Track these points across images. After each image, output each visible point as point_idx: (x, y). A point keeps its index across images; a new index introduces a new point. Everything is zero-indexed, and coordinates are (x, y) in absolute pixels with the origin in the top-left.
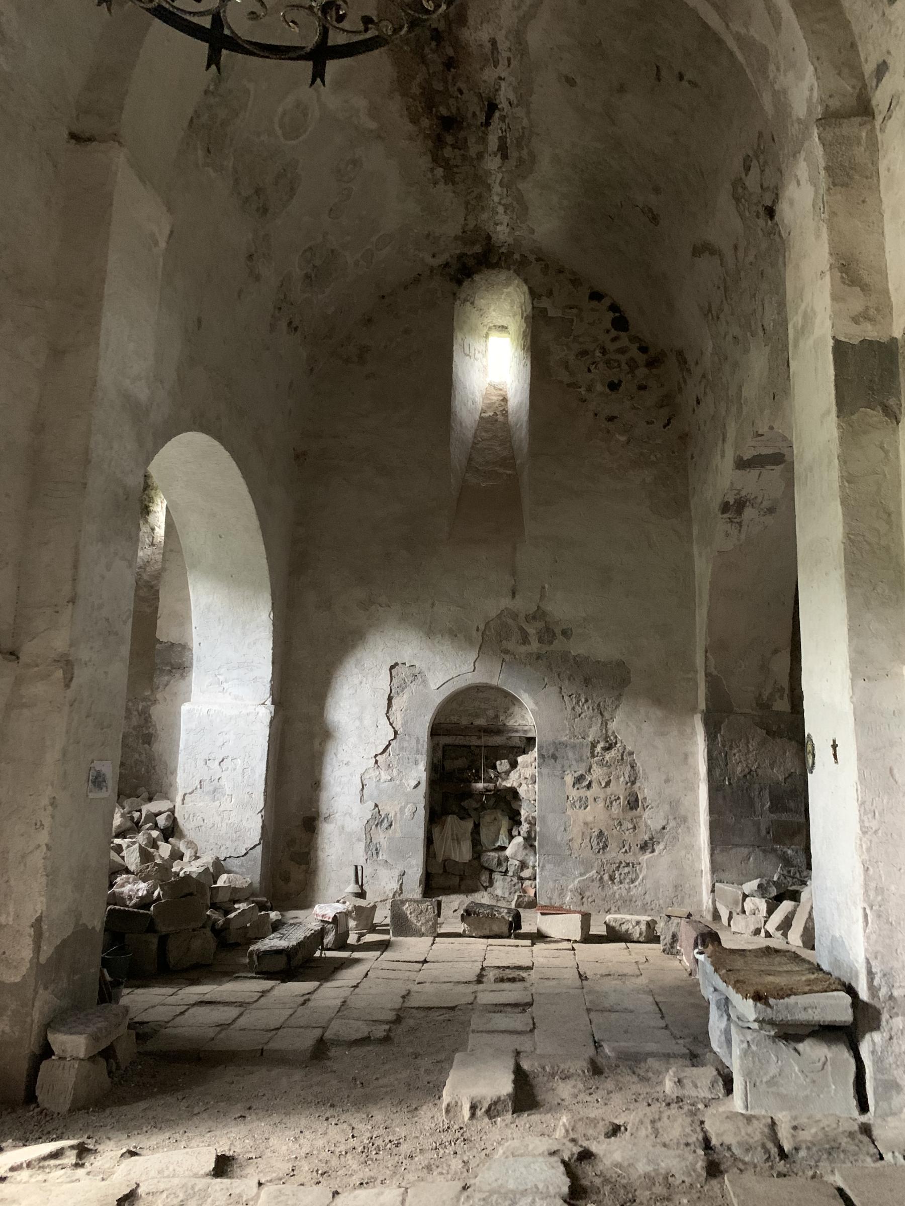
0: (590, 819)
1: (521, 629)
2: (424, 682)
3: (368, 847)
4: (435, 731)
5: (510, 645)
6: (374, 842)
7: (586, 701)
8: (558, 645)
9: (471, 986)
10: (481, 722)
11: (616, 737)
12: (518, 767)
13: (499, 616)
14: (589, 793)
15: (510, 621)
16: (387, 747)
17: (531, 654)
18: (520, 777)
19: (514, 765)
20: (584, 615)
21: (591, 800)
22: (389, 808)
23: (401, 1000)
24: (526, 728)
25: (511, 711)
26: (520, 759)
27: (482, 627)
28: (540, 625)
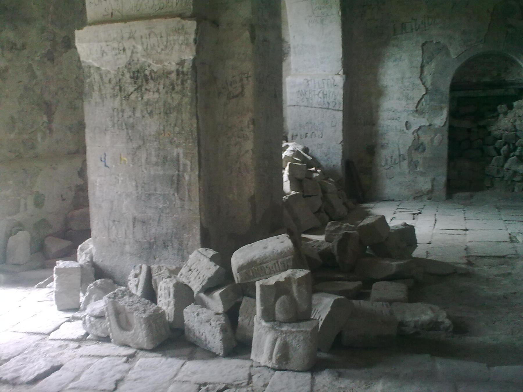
2: (448, 54)
3: (409, 163)
4: (454, 87)
6: (414, 160)
9: (506, 243)
10: (487, 79)
16: (421, 99)
18: (515, 116)
19: (511, 107)
22: (425, 139)
23: (465, 251)
26: (515, 104)
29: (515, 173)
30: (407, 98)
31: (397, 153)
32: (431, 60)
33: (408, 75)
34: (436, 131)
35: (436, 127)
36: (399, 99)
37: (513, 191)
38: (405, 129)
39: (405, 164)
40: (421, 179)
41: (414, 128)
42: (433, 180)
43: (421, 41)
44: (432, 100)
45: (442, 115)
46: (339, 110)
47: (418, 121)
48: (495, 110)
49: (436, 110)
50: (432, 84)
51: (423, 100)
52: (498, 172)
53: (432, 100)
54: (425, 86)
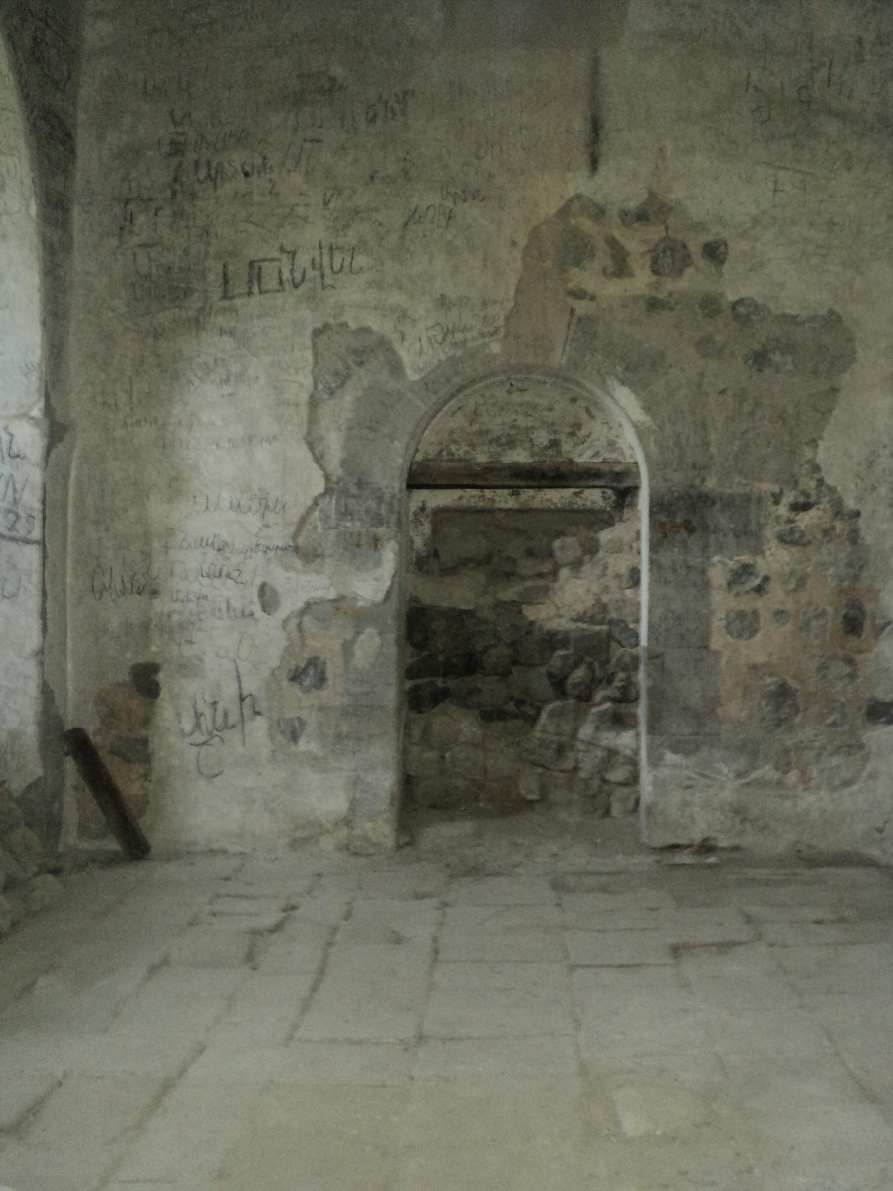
0: (759, 658)
1: (612, 242)
5: (586, 278)
7: (757, 404)
8: (692, 281)
10: (520, 456)
11: (821, 482)
12: (601, 554)
13: (564, 212)
14: (759, 604)
15: (587, 225)
16: (310, 510)
17: (635, 299)
19: (591, 549)
20: (753, 211)
21: (765, 616)
24: (618, 469)
25: (583, 432)
26: (605, 536)
27: (523, 241)
28: (655, 233)
29: (612, 753)
30: (265, 507)
31: (230, 690)
32: (343, 384)
33: (267, 426)
34: (361, 618)
35: (361, 604)
36: (237, 507)
37: (607, 812)
38: (257, 609)
39: (259, 727)
40: (312, 778)
41: (290, 605)
42: (355, 782)
43: (311, 318)
44: (346, 513)
45: (378, 564)
46: (27, 542)
47: (303, 586)
48: (550, 554)
49: (360, 549)
50: (344, 463)
51: (317, 513)
52: (561, 750)
53: (346, 513)
54: (322, 468)
